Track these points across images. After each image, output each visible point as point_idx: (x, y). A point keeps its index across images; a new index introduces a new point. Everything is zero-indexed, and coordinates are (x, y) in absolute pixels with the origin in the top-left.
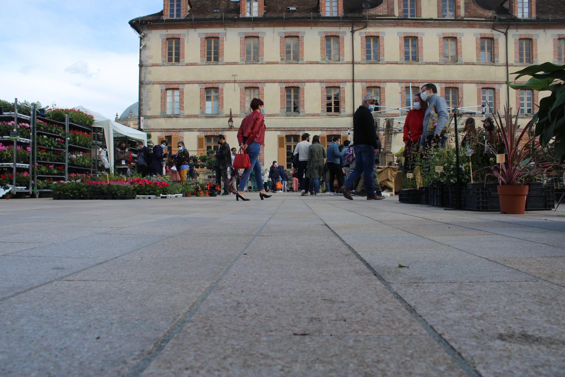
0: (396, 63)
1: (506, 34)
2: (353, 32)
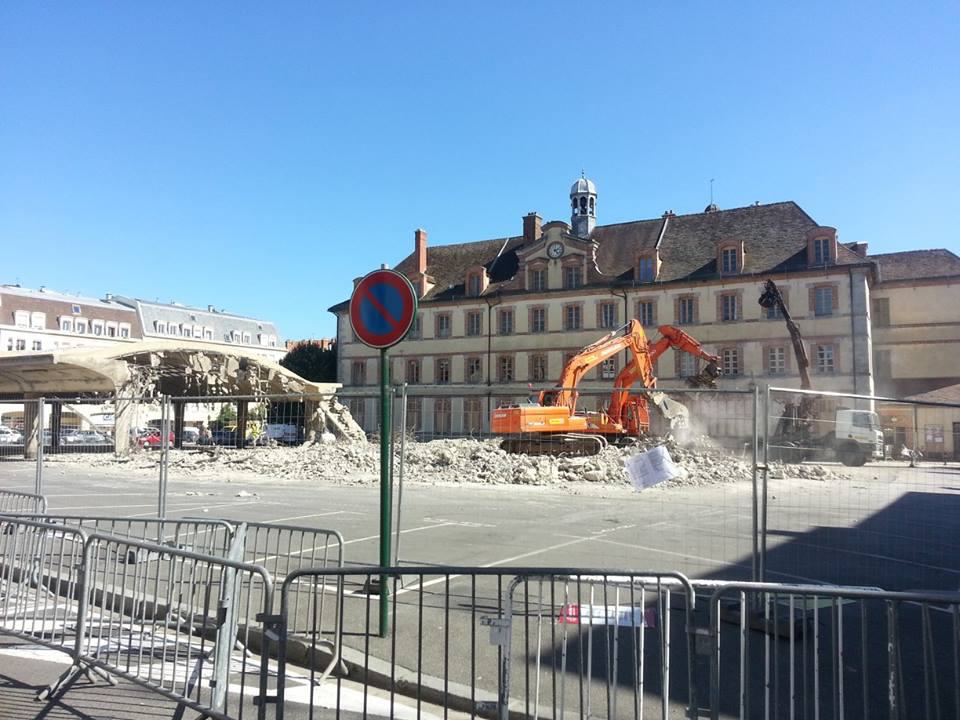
0: (525, 334)
1: (626, 298)
2: (490, 308)
